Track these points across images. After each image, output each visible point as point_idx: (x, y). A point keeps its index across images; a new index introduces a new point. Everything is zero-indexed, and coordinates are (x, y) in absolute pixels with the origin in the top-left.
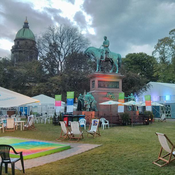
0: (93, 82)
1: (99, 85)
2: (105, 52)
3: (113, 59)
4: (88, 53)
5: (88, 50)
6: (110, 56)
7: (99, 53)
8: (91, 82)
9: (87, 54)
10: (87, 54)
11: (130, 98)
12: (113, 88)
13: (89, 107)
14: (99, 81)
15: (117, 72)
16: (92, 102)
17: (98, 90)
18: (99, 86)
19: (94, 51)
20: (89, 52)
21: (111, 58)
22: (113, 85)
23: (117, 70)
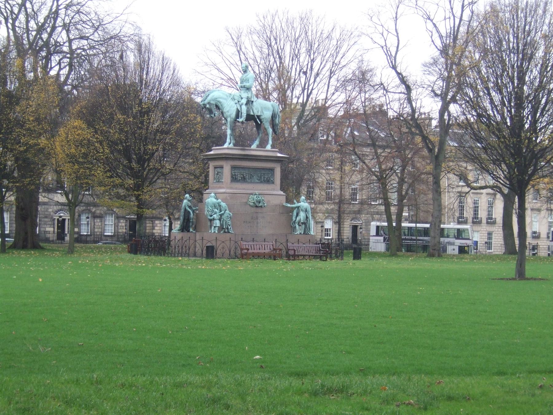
0: (219, 170)
1: (232, 177)
2: (244, 101)
3: (262, 117)
4: (209, 103)
5: (209, 98)
6: (255, 111)
7: (232, 103)
8: (211, 170)
9: (208, 106)
10: (208, 106)
11: (298, 207)
12: (261, 182)
13: (218, 225)
14: (233, 168)
15: (269, 147)
16: (223, 214)
17: (231, 188)
18: (234, 179)
19: (221, 100)
20: (212, 102)
21: (259, 114)
22: (261, 177)
23: (270, 142)
